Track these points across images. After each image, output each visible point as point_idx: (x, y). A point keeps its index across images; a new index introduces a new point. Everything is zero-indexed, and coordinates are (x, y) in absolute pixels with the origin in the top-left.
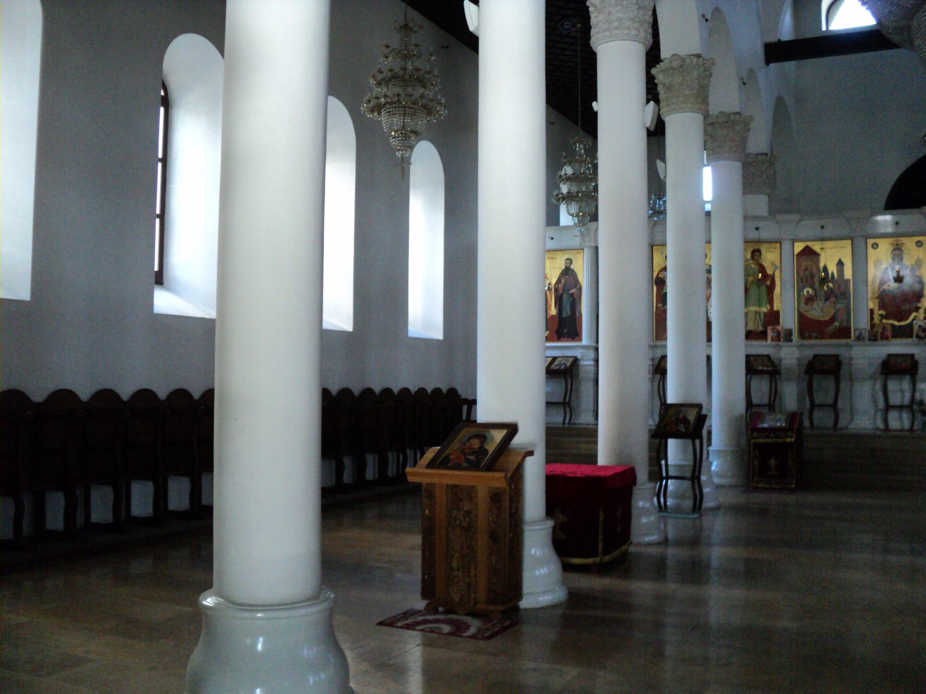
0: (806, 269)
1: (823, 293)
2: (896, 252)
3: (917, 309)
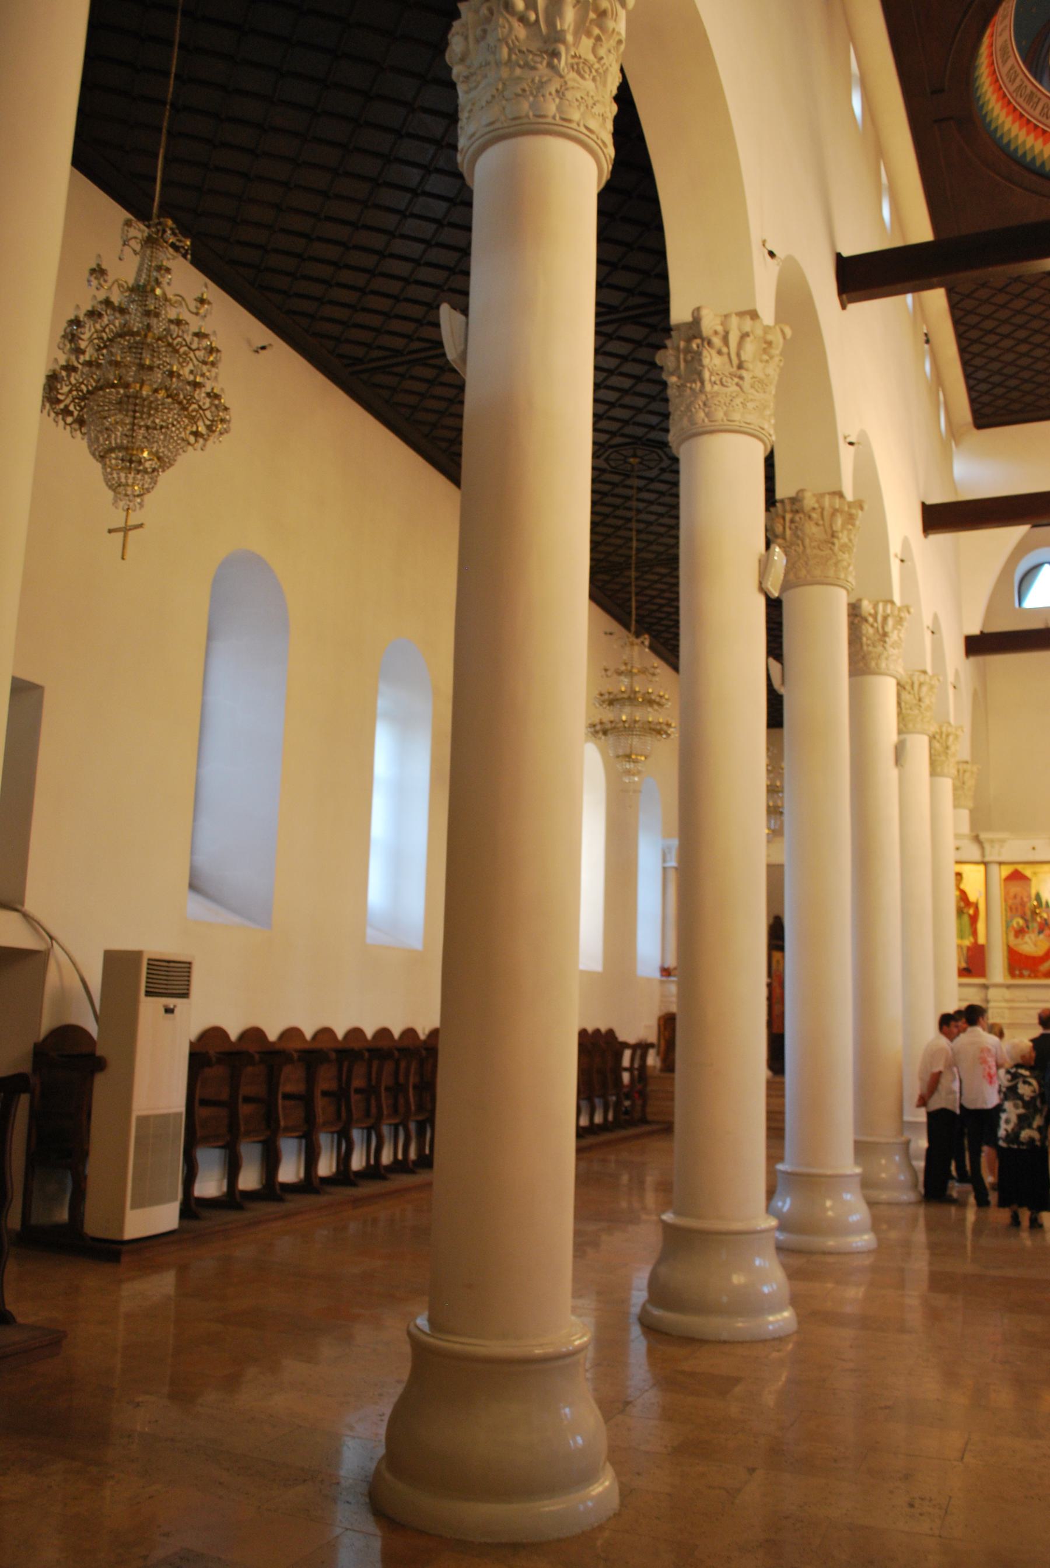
0: (1015, 897)
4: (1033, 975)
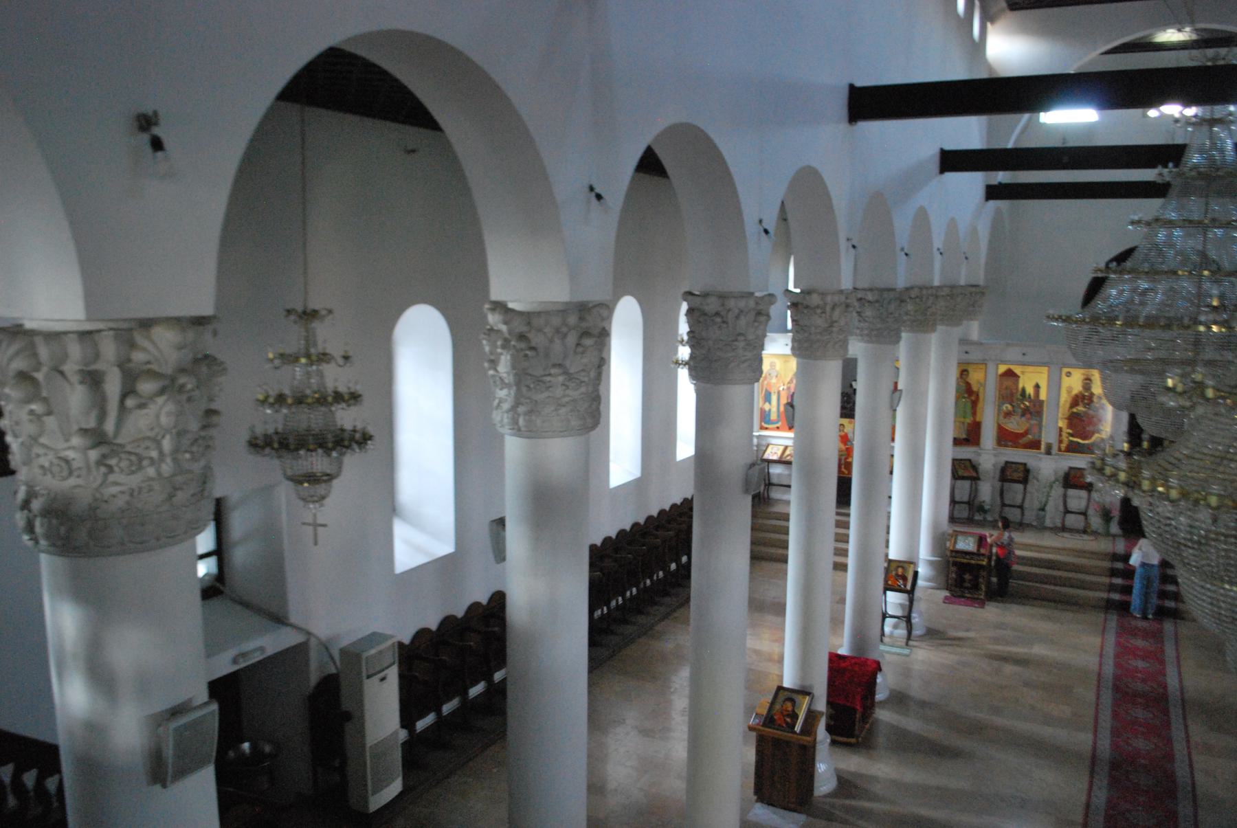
0: (1006, 388)
1: (1020, 410)
2: (1088, 381)
3: (1098, 432)
4: (1014, 445)
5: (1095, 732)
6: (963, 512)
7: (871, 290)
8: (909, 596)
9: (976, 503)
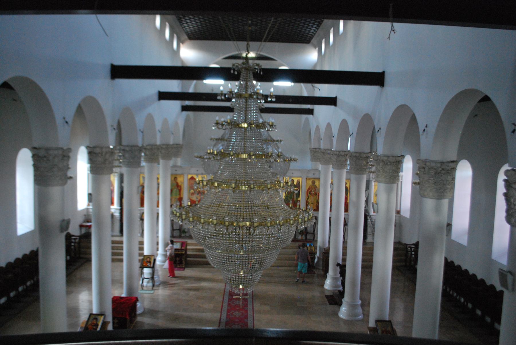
5: (221, 312)
6: (177, 233)
7: (128, 146)
8: (152, 270)
9: (182, 229)
